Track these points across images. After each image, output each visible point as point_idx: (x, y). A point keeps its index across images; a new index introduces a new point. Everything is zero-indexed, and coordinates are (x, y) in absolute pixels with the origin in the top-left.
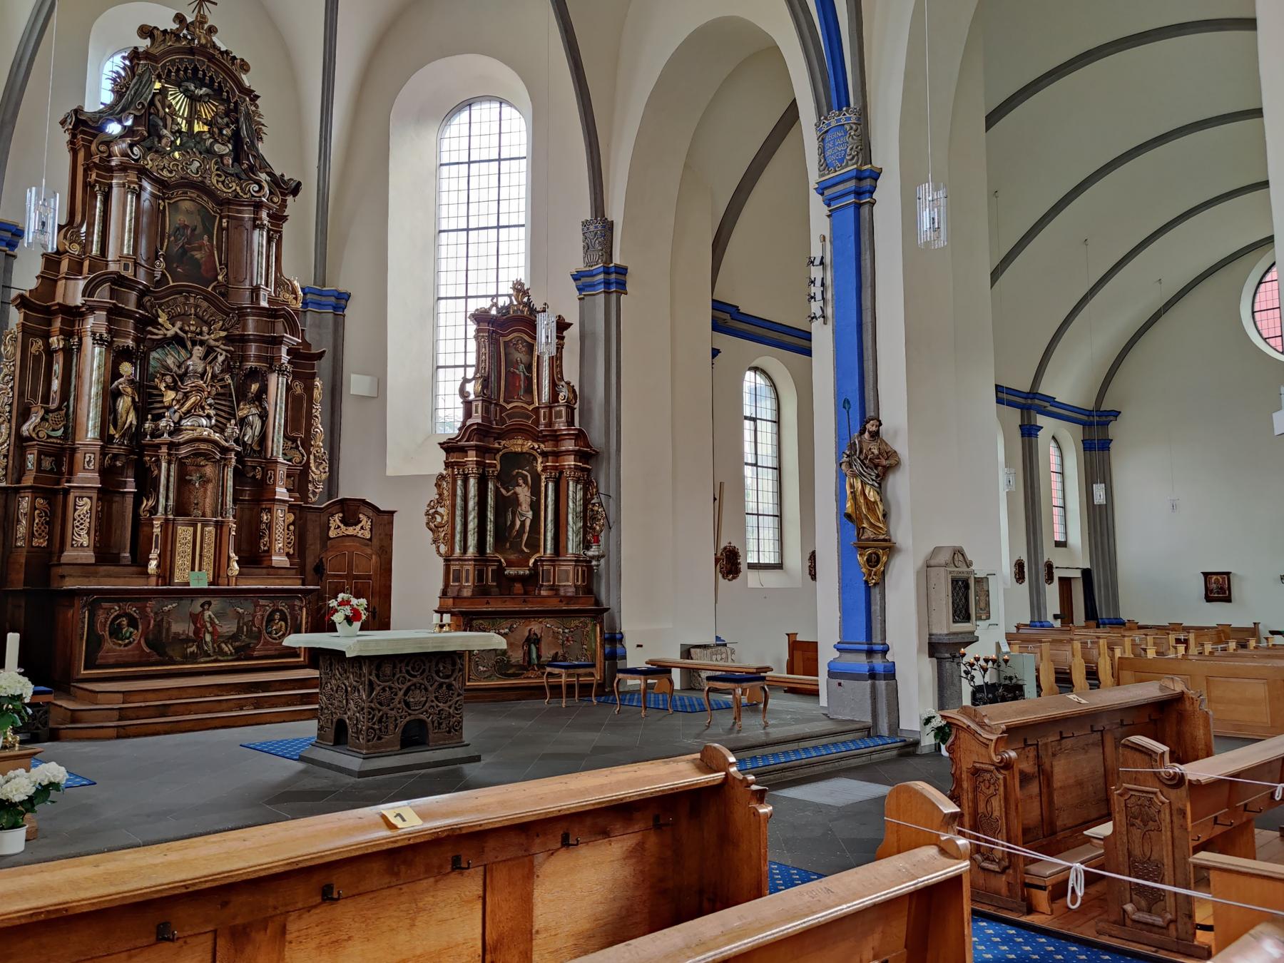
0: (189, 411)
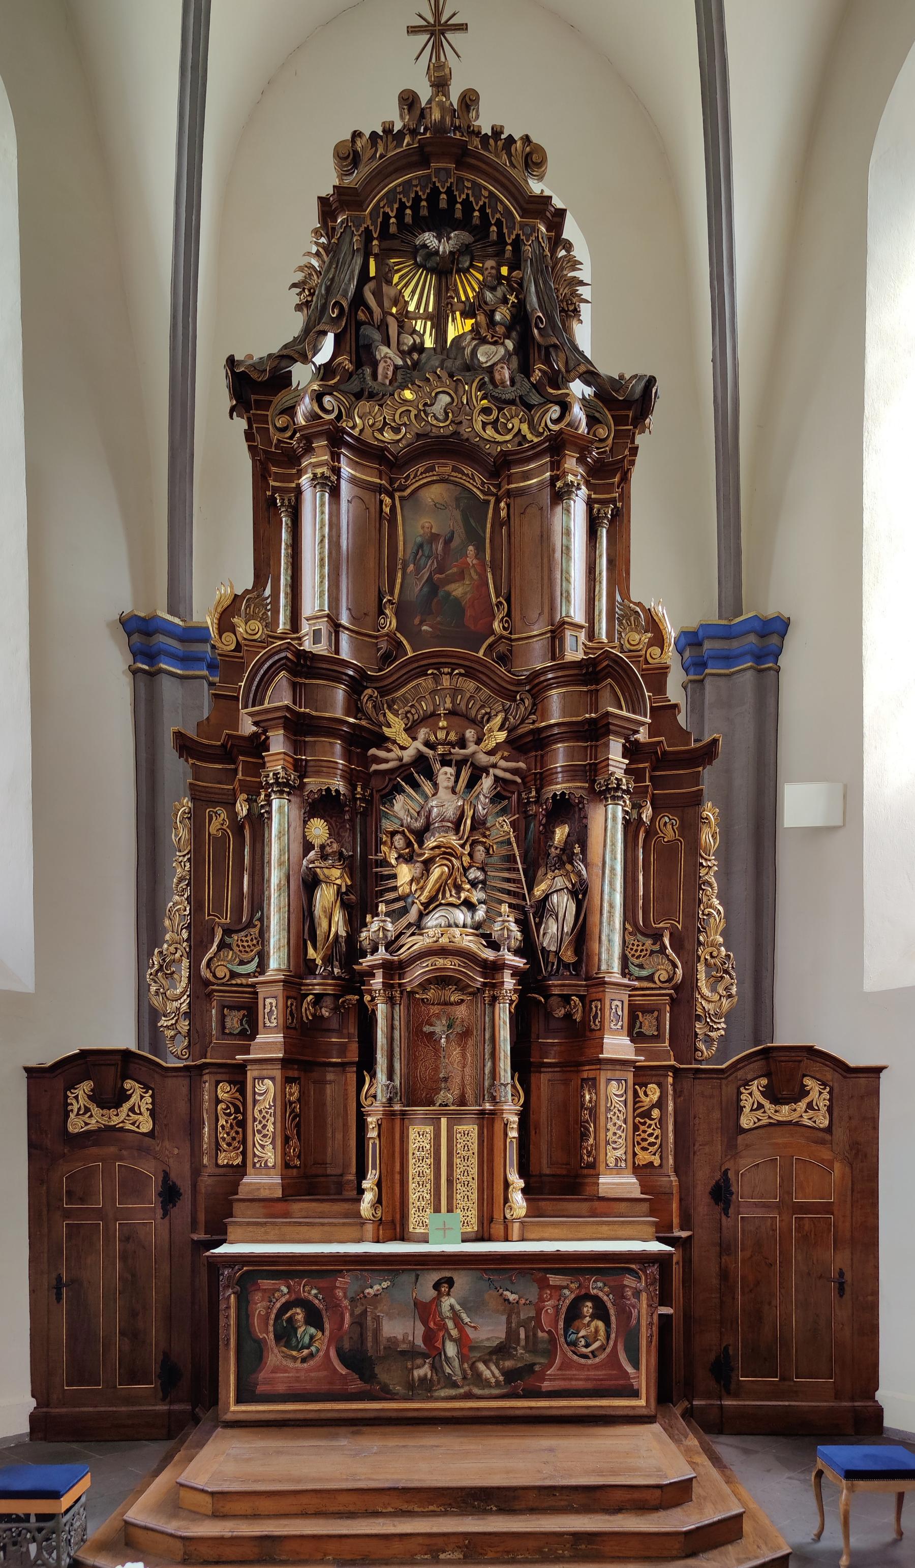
0: (432, 899)
